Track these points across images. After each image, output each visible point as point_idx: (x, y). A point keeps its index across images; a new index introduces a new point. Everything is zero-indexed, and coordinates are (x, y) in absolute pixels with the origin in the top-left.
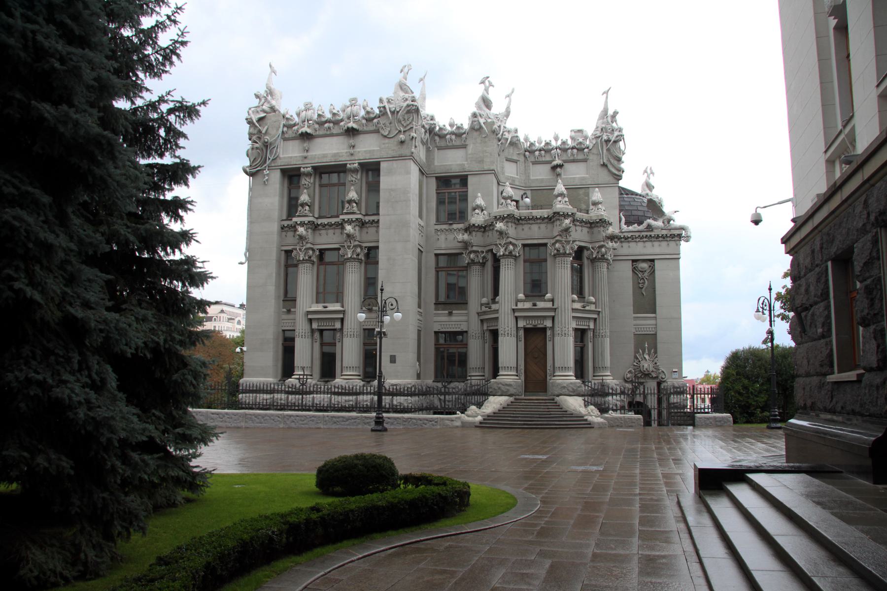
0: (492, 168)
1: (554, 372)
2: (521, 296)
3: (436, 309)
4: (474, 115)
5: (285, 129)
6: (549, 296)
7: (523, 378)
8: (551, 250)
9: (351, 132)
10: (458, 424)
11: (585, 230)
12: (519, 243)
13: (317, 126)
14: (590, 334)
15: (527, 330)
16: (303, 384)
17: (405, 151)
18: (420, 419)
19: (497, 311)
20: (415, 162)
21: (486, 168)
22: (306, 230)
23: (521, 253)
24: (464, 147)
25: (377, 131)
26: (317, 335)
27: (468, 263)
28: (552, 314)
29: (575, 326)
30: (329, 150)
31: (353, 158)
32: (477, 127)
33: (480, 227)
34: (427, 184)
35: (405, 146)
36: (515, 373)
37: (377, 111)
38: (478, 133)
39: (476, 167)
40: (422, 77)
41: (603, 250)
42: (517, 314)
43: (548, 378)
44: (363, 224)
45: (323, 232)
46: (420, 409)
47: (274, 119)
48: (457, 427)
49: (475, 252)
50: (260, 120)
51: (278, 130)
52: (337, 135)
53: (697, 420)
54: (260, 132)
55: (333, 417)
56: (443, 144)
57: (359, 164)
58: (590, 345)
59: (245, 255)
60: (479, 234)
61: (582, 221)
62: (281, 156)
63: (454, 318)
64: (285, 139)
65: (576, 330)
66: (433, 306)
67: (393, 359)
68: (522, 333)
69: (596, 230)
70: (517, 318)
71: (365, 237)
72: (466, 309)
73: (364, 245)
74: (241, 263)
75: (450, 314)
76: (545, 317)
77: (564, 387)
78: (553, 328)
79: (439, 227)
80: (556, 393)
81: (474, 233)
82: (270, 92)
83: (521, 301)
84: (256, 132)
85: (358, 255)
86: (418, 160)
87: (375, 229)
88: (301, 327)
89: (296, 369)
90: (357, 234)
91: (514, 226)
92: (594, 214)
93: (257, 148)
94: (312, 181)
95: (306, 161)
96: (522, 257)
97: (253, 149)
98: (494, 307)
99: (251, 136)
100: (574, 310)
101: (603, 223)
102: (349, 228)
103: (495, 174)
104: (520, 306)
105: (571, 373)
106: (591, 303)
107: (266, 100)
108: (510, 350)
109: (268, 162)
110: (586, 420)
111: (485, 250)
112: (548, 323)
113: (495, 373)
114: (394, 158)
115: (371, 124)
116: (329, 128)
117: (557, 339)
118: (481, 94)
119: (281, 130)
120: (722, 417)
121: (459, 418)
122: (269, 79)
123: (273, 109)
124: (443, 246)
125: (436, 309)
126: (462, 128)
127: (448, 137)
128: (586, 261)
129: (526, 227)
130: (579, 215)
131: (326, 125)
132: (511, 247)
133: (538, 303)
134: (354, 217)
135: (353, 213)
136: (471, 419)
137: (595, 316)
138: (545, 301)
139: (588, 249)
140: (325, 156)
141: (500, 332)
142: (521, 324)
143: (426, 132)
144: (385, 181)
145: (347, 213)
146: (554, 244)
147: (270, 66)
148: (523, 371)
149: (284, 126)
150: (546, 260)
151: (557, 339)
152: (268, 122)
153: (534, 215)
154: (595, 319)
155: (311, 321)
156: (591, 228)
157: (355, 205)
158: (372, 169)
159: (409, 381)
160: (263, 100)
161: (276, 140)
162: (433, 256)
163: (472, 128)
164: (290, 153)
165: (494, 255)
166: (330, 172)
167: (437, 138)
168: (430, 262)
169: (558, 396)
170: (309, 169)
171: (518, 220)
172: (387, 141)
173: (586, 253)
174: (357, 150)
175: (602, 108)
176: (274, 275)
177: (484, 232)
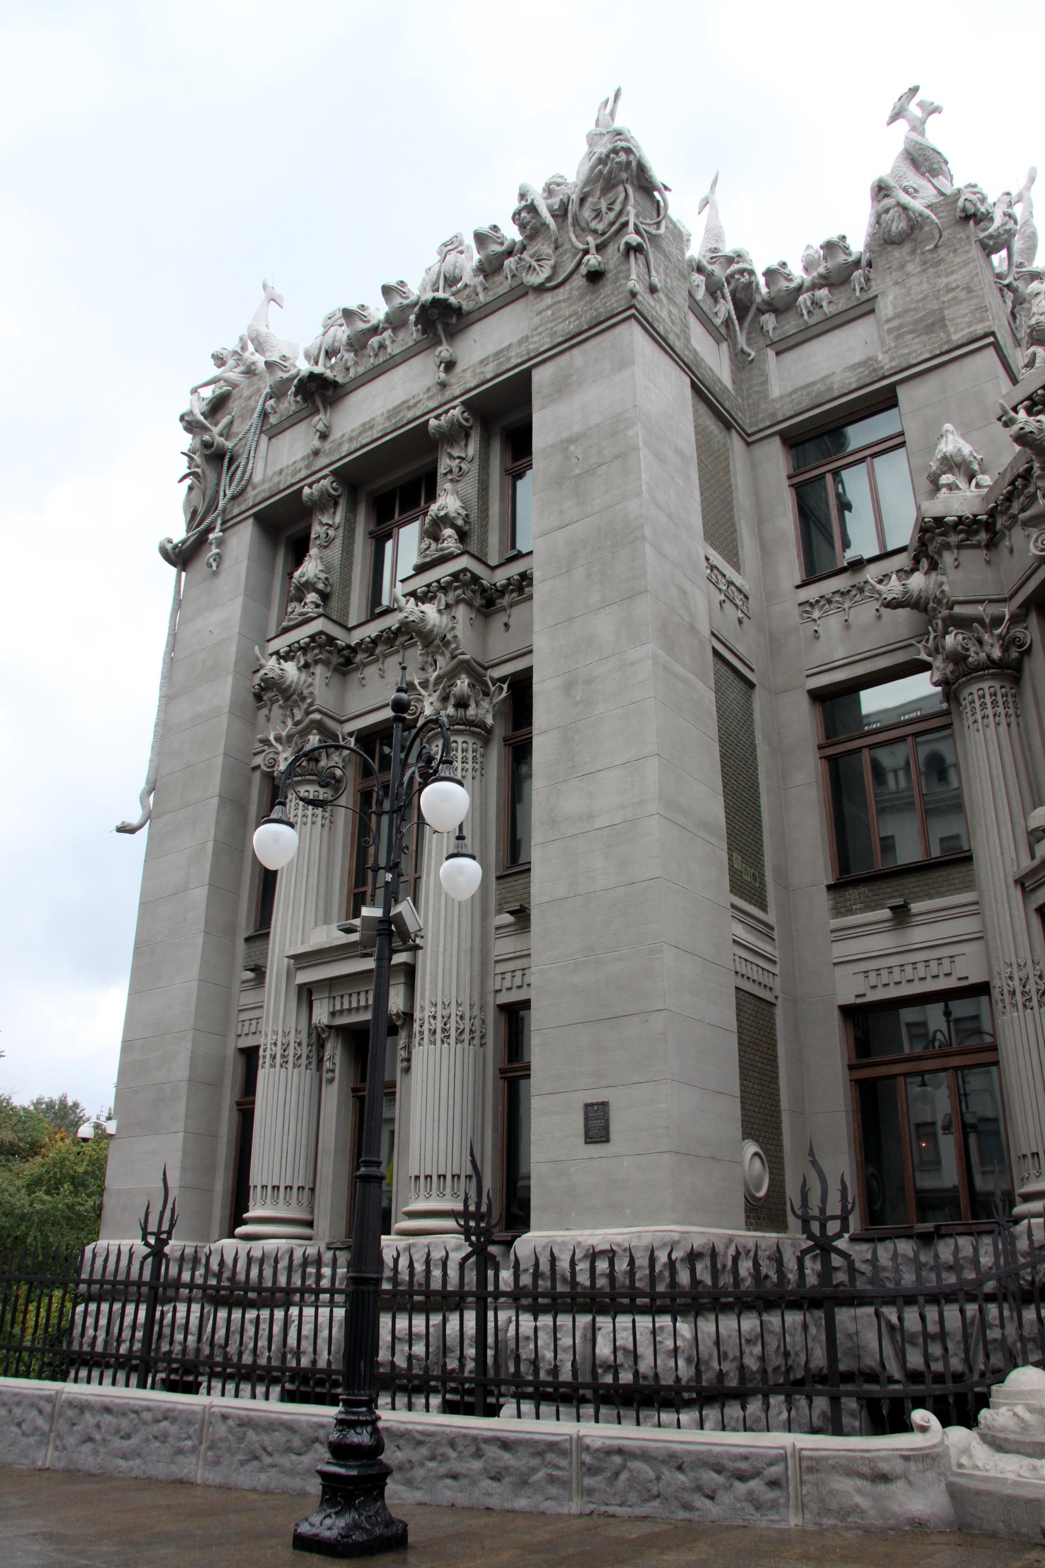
0: (980, 329)
3: (838, 911)
4: (881, 190)
9: (439, 319)
10: (921, 1501)
16: (157, 1253)
17: (609, 298)
18: (677, 1462)
21: (957, 337)
24: (866, 309)
25: (520, 292)
26: (334, 1052)
31: (448, 394)
32: (898, 226)
33: (967, 526)
34: (753, 466)
35: (607, 288)
37: (512, 233)
38: (907, 247)
39: (918, 349)
40: (705, 191)
44: (490, 603)
45: (371, 671)
46: (706, 1393)
48: (919, 1526)
49: (963, 623)
52: (407, 355)
55: (246, 1423)
56: (791, 325)
59: (143, 799)
60: (973, 558)
62: (257, 478)
63: (918, 935)
66: (822, 900)
67: (597, 1126)
71: (500, 644)
72: (969, 885)
73: (497, 673)
74: (125, 829)
75: (901, 916)
79: (812, 592)
81: (948, 558)
85: (462, 704)
86: (678, 345)
88: (276, 1021)
94: (338, 518)
95: (322, 461)
103: (996, 346)
111: (1007, 610)
114: (574, 340)
115: (498, 279)
116: (382, 346)
118: (900, 147)
119: (259, 408)
121: (929, 1458)
124: (839, 653)
125: (838, 911)
126: (846, 250)
127: (804, 298)
131: (374, 341)
136: (1010, 1469)
140: (368, 426)
143: (714, 291)
152: (235, 406)
155: (307, 993)
159: (672, 1230)
162: (804, 703)
163: (885, 240)
164: (282, 461)
167: (769, 321)
168: (790, 728)
172: (548, 299)
176: (210, 845)
177: (991, 545)
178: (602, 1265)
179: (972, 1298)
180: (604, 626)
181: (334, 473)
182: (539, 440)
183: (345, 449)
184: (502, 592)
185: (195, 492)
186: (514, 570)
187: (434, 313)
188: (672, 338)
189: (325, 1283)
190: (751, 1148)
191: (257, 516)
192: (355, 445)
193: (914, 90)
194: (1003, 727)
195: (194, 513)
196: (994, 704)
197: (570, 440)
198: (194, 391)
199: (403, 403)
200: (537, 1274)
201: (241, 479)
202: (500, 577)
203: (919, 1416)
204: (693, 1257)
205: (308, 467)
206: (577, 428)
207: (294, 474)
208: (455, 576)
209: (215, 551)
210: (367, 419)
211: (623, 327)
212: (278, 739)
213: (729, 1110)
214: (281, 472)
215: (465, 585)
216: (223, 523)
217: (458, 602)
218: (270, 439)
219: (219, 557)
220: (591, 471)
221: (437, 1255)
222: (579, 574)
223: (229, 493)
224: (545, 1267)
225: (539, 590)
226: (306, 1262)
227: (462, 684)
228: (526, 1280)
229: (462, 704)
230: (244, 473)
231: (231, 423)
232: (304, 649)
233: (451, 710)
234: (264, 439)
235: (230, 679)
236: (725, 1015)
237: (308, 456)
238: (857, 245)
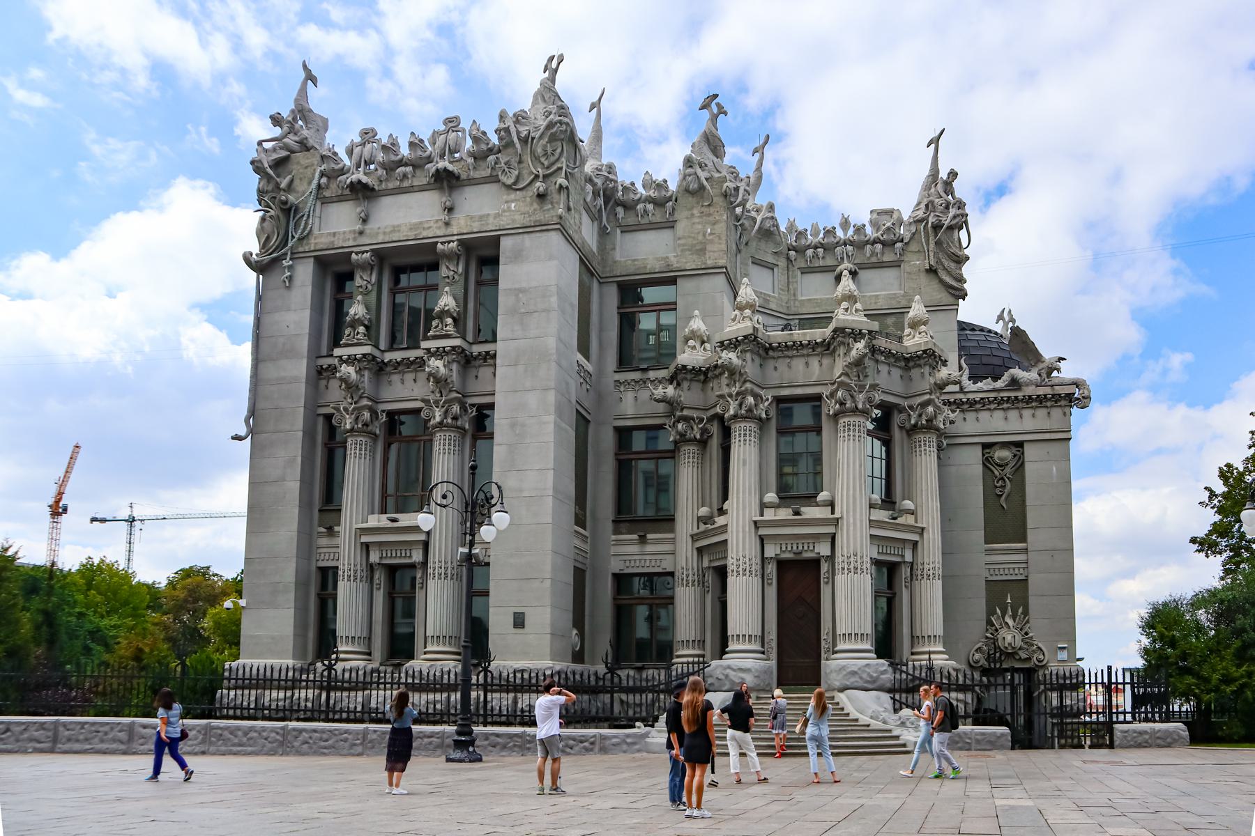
1: (834, 645)
2: (771, 497)
5: (324, 180)
6: (823, 496)
7: (774, 655)
8: (830, 407)
11: (896, 373)
12: (769, 395)
13: (381, 172)
14: (905, 572)
15: (782, 564)
19: (724, 529)
20: (569, 239)
22: (358, 372)
23: (773, 413)
27: (675, 442)
28: (831, 530)
29: (875, 556)
30: (408, 217)
31: (449, 231)
36: (757, 647)
41: (930, 409)
42: (762, 532)
47: (304, 162)
50: (279, 164)
51: (310, 183)
52: (422, 189)
53: (1117, 734)
54: (277, 186)
57: (461, 242)
58: (905, 595)
61: (889, 354)
62: (316, 232)
64: (325, 201)
65: (877, 563)
67: (519, 621)
68: (771, 569)
69: (915, 373)
70: (762, 539)
76: (817, 537)
77: (854, 673)
78: (831, 558)
80: (837, 684)
82: (302, 111)
84: (270, 188)
86: (576, 237)
87: (489, 370)
90: (455, 377)
91: (757, 360)
92: (913, 342)
93: (271, 217)
96: (773, 423)
97: (263, 219)
98: (720, 521)
99: (261, 192)
100: (873, 524)
101: (931, 358)
102: (436, 364)
104: (769, 515)
105: (868, 646)
107: (292, 130)
108: (748, 604)
109: (290, 244)
110: (897, 737)
112: (824, 549)
113: (722, 650)
119: (315, 182)
120: (1167, 731)
122: (303, 92)
123: (305, 146)
128: (897, 434)
129: (782, 364)
130: (882, 343)
132: (751, 400)
133: (803, 509)
135: (447, 336)
137: (915, 537)
138: (818, 506)
139: (901, 410)
140: (395, 229)
141: (731, 567)
142: (771, 551)
144: (509, 275)
145: (435, 337)
146: (832, 395)
147: (305, 66)
148: (774, 644)
149: (322, 174)
150: (818, 430)
151: (838, 577)
153: (796, 338)
154: (915, 544)
156: (907, 368)
157: (449, 320)
158: (483, 256)
159: (550, 663)
160: (286, 128)
161: (304, 202)
165: (720, 418)
166: (408, 264)
169: (842, 690)
170: (367, 255)
171: (766, 350)
173: (897, 419)
174: (456, 215)
175: (927, 172)
178: (519, 675)
179: (653, 691)
180: (532, 399)
184: (475, 358)
185: (265, 225)
186: (483, 348)
187: (444, 175)
190: (575, 632)
195: (268, 239)
197: (521, 290)
198: (260, 143)
199: (421, 223)
201: (305, 228)
202: (476, 349)
203: (638, 724)
204: (559, 673)
205: (355, 239)
206: (524, 285)
207: (344, 241)
209: (288, 274)
210: (396, 223)
211: (553, 233)
212: (346, 409)
213: (569, 616)
214: (334, 234)
215: (459, 354)
217: (454, 361)
219: (290, 278)
220: (529, 313)
221: (446, 669)
222: (521, 368)
223: (297, 237)
227: (456, 409)
229: (455, 418)
230: (306, 224)
231: (292, 181)
232: (359, 361)
233: (449, 421)
234: (319, 203)
235: (305, 361)
236: (569, 578)
237: (354, 232)
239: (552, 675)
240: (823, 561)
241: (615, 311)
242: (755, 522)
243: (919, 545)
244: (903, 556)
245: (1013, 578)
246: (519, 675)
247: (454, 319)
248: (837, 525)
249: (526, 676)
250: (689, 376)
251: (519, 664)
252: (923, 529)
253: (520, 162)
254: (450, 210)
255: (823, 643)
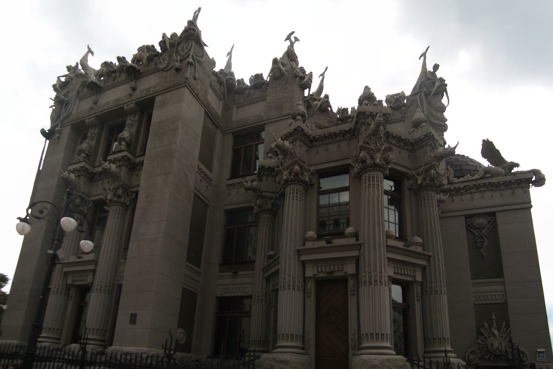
1: (360, 343)
2: (311, 234)
14: (417, 290)
15: (320, 283)
28: (356, 253)
29: (392, 274)
36: (301, 345)
42: (303, 258)
43: (351, 352)
62: (74, 112)
68: (311, 285)
70: (304, 264)
78: (356, 275)
83: (311, 239)
89: (44, 330)
91: (304, 148)
95: (93, 112)
106: (417, 244)
112: (350, 269)
117: (363, 290)
133: (333, 241)
134: (119, 155)
137: (424, 263)
142: (310, 272)
145: (115, 153)
148: (312, 342)
151: (361, 290)
154: (424, 268)
159: (145, 349)
170: (92, 119)
181: (96, 116)
182: (153, 120)
183: (100, 109)
188: (200, 95)
189: (58, 356)
191: (72, 125)
192: (103, 109)
193: (293, 33)
194: (268, 228)
196: (267, 221)
200: (111, 357)
208: (123, 157)
216: (61, 125)
217: (123, 165)
218: (80, 100)
224: (114, 356)
225: (145, 166)
226: (53, 350)
228: (108, 359)
238: (266, 77)
239: (147, 358)
240: (349, 277)
241: (231, 148)
242: (298, 251)
243: (427, 268)
244: (414, 277)
245: (496, 302)
246: (124, 356)
247: (127, 143)
248: (360, 250)
249: (128, 357)
250: (266, 173)
251: (126, 349)
252: (429, 256)
253: (170, 57)
254: (134, 89)
255: (350, 341)
